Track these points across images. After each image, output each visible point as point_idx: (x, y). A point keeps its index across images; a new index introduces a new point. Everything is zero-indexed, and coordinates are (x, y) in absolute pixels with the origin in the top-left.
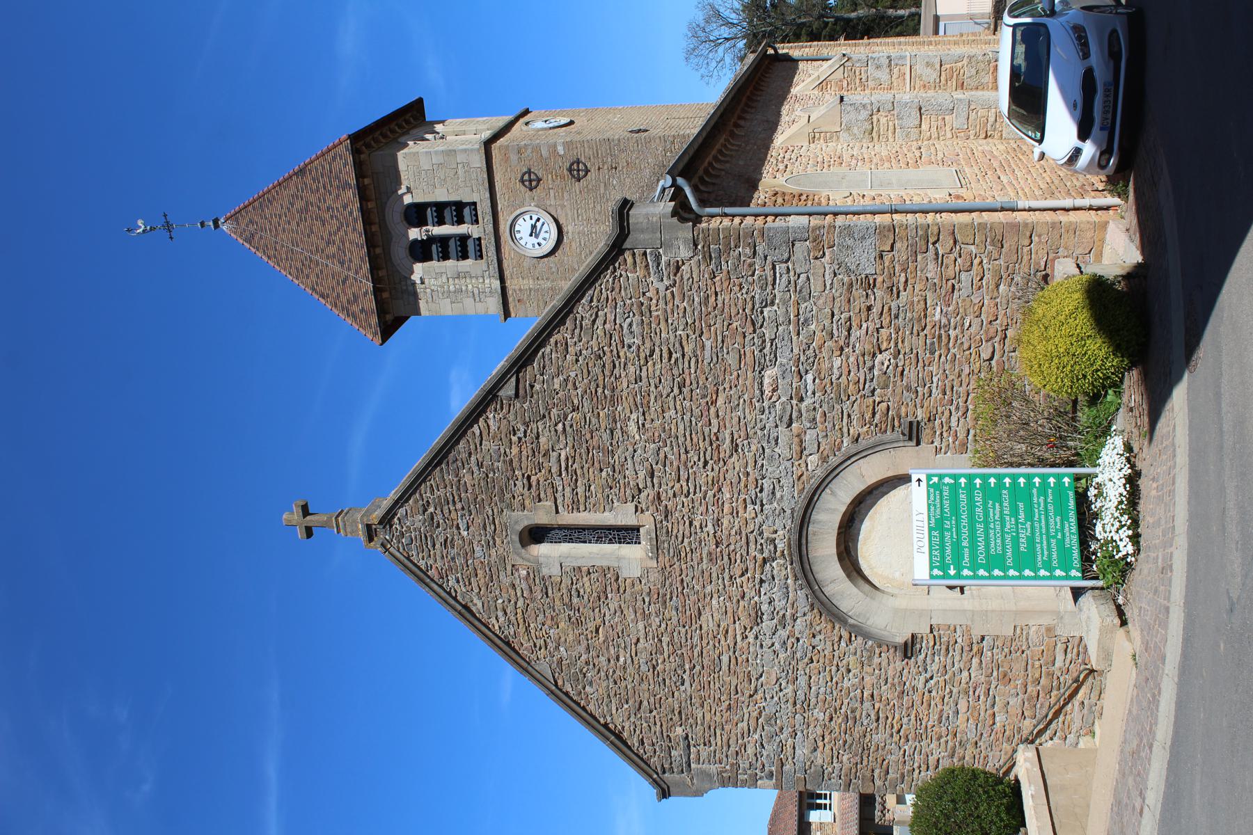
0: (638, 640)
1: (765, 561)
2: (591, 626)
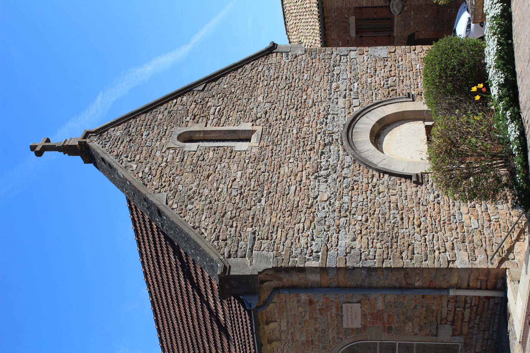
0: (235, 179)
1: (325, 145)
2: (206, 173)
